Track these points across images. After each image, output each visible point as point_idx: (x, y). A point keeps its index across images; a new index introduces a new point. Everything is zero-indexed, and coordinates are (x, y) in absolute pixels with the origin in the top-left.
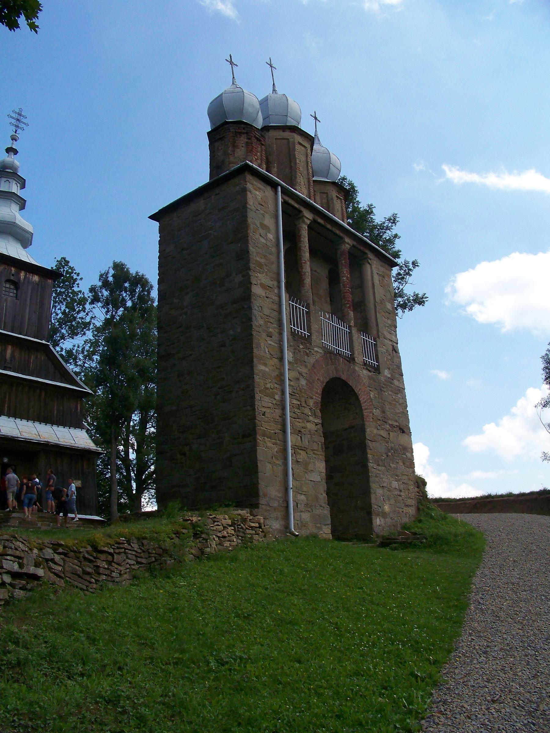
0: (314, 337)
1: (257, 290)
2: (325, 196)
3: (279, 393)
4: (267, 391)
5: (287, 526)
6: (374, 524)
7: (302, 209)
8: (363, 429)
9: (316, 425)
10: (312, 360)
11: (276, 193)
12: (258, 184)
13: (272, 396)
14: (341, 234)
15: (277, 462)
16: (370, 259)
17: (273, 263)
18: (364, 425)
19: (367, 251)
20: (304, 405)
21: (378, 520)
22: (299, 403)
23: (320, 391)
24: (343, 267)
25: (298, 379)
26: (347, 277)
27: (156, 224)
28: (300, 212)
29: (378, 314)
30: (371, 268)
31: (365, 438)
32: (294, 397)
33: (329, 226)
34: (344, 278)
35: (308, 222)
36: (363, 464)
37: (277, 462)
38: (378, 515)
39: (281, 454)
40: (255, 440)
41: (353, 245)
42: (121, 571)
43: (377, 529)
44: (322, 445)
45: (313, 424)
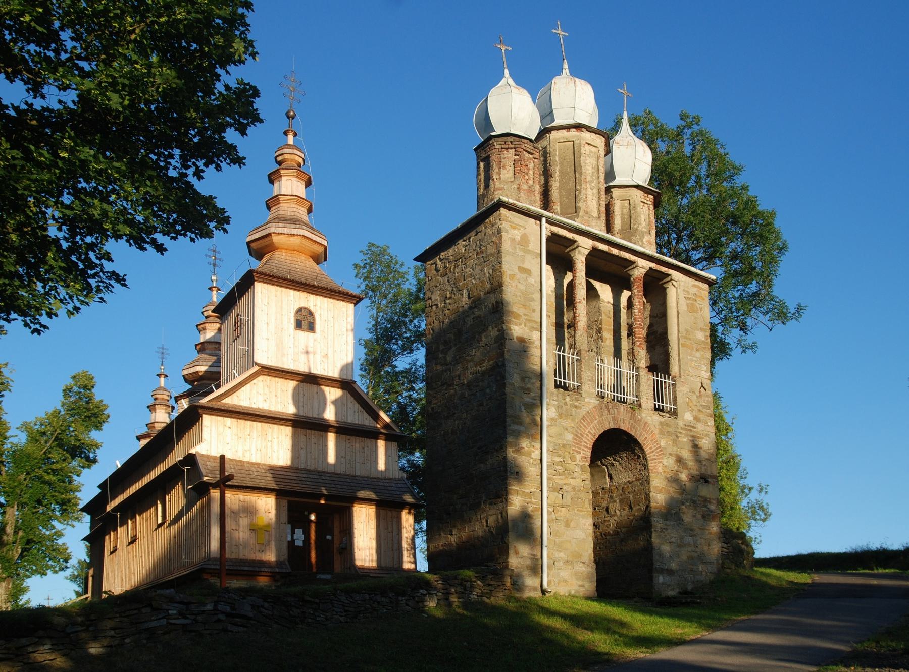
0: (585, 388)
10: (583, 411)
23: (590, 444)
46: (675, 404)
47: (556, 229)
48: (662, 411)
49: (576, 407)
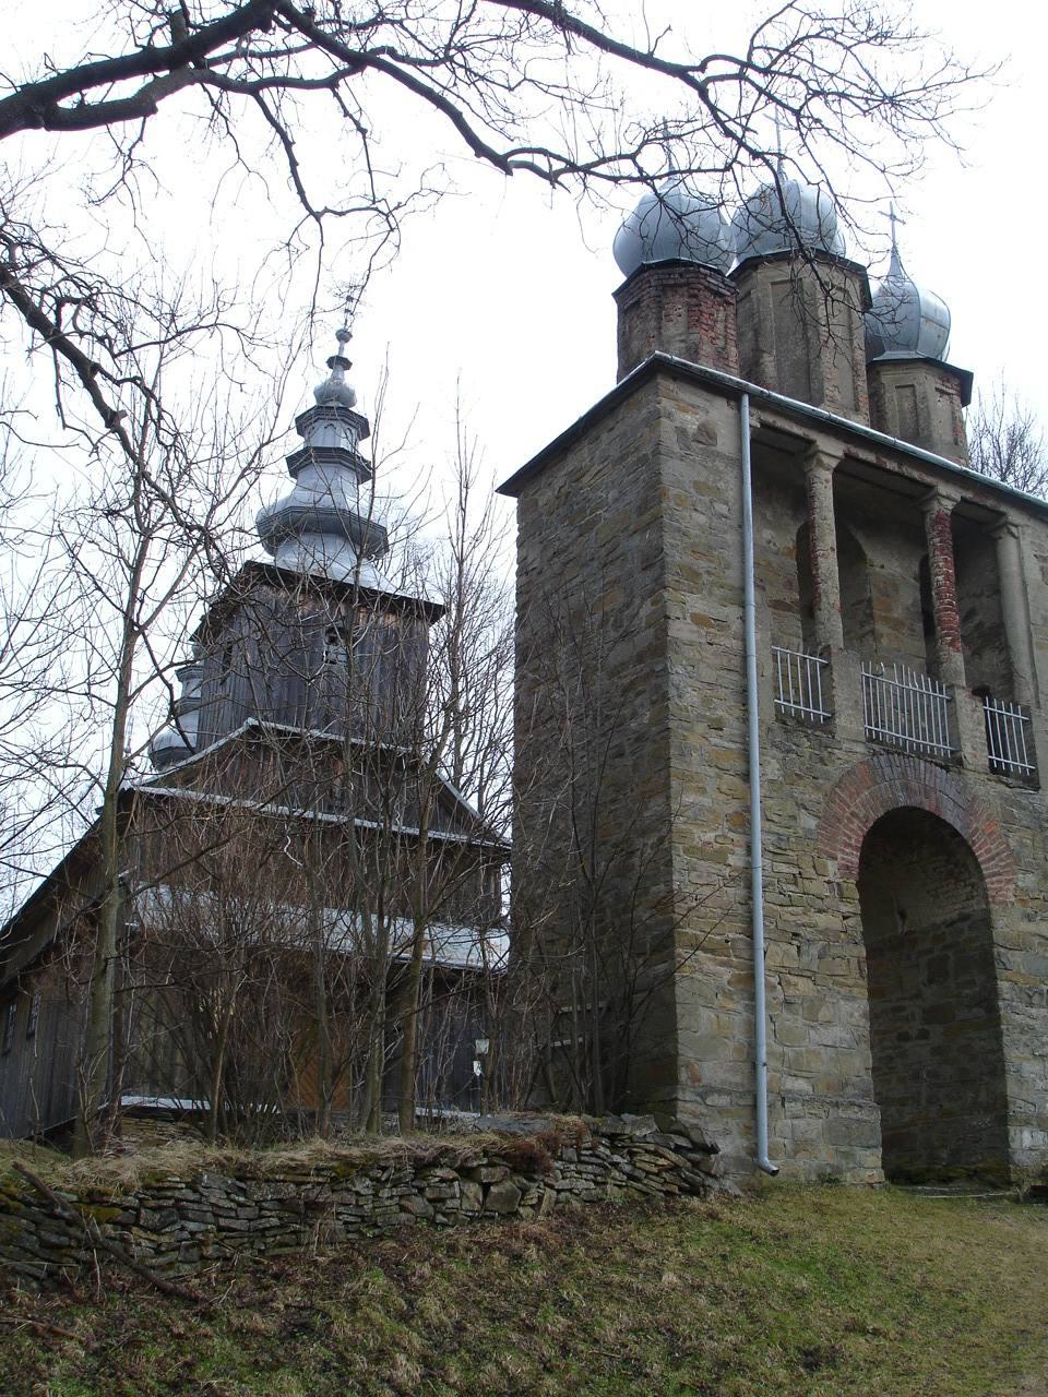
1: (680, 630)
2: (908, 392)
3: (740, 851)
4: (708, 848)
5: (754, 1152)
6: (1014, 1145)
7: (813, 435)
8: (986, 922)
9: (845, 918)
10: (834, 770)
11: (739, 408)
12: (689, 395)
13: (720, 857)
14: (929, 479)
15: (731, 1005)
16: (1016, 526)
17: (728, 567)
18: (988, 912)
19: (1003, 508)
20: (810, 872)
21: (1026, 1135)
22: (796, 871)
23: (857, 840)
24: (937, 553)
25: (794, 818)
26: (947, 575)
27: (511, 503)
28: (811, 442)
29: (1036, 652)
30: (1019, 545)
31: (992, 944)
32: (778, 858)
33: (891, 465)
34: (940, 578)
35: (834, 463)
36: (988, 1001)
37: (731, 1005)
38: (1027, 1123)
39: (741, 986)
40: (672, 957)
41: (964, 499)
42: (160, 1245)
43: (1021, 1158)
44: (859, 962)
45: (839, 916)
46: (1033, 758)
47: (770, 419)
48: (1007, 773)
49: (822, 760)
